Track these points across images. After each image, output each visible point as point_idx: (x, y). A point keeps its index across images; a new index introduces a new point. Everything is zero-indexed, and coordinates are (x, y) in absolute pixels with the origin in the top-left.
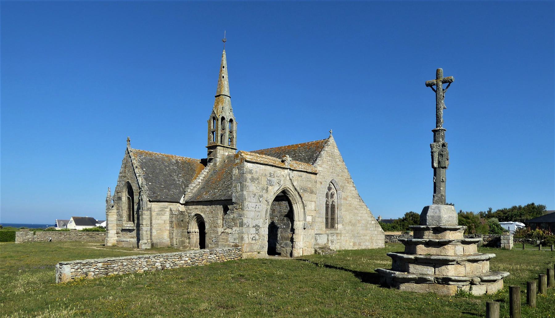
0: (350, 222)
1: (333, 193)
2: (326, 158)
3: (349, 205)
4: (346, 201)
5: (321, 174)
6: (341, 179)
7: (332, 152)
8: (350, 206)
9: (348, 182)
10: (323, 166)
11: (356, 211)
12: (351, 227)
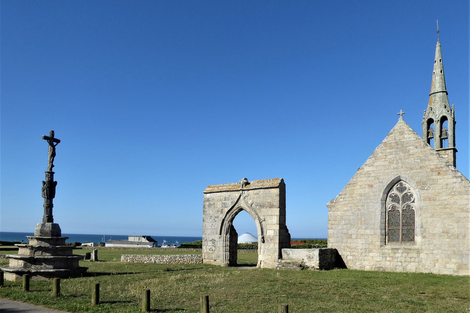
0: (443, 232)
1: (409, 194)
2: (381, 153)
3: (441, 206)
4: (432, 202)
5: (372, 175)
6: (418, 172)
7: (398, 141)
8: (445, 208)
9: (439, 173)
10: (376, 164)
11: (463, 215)
12: (448, 240)
